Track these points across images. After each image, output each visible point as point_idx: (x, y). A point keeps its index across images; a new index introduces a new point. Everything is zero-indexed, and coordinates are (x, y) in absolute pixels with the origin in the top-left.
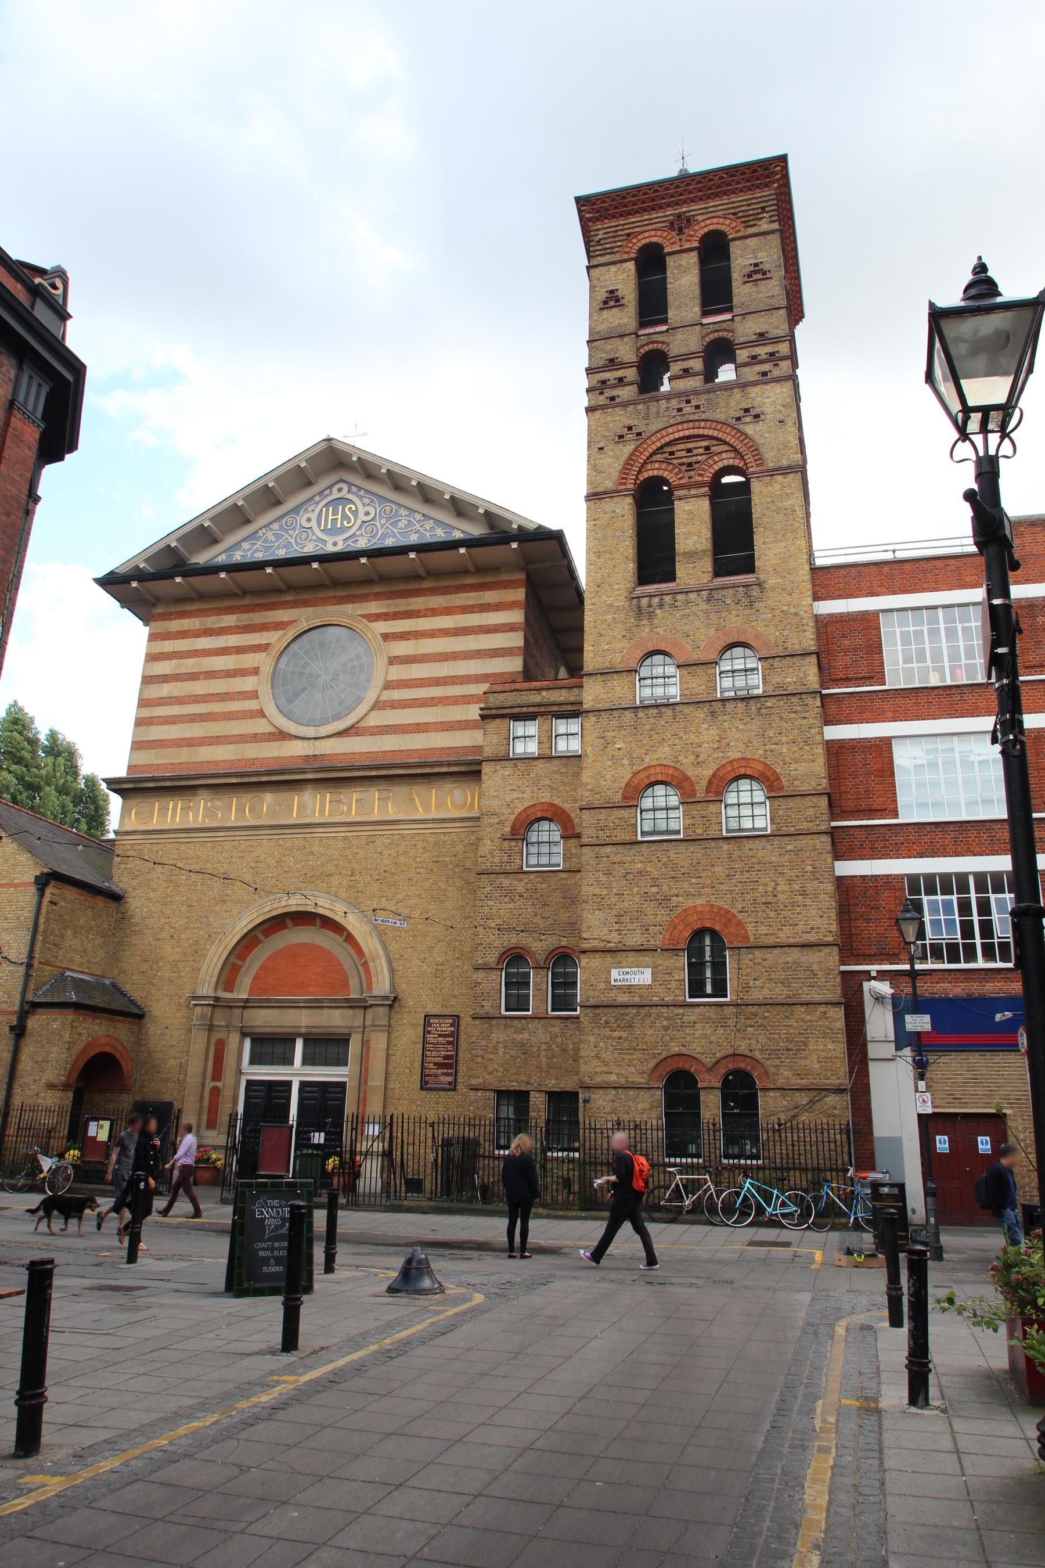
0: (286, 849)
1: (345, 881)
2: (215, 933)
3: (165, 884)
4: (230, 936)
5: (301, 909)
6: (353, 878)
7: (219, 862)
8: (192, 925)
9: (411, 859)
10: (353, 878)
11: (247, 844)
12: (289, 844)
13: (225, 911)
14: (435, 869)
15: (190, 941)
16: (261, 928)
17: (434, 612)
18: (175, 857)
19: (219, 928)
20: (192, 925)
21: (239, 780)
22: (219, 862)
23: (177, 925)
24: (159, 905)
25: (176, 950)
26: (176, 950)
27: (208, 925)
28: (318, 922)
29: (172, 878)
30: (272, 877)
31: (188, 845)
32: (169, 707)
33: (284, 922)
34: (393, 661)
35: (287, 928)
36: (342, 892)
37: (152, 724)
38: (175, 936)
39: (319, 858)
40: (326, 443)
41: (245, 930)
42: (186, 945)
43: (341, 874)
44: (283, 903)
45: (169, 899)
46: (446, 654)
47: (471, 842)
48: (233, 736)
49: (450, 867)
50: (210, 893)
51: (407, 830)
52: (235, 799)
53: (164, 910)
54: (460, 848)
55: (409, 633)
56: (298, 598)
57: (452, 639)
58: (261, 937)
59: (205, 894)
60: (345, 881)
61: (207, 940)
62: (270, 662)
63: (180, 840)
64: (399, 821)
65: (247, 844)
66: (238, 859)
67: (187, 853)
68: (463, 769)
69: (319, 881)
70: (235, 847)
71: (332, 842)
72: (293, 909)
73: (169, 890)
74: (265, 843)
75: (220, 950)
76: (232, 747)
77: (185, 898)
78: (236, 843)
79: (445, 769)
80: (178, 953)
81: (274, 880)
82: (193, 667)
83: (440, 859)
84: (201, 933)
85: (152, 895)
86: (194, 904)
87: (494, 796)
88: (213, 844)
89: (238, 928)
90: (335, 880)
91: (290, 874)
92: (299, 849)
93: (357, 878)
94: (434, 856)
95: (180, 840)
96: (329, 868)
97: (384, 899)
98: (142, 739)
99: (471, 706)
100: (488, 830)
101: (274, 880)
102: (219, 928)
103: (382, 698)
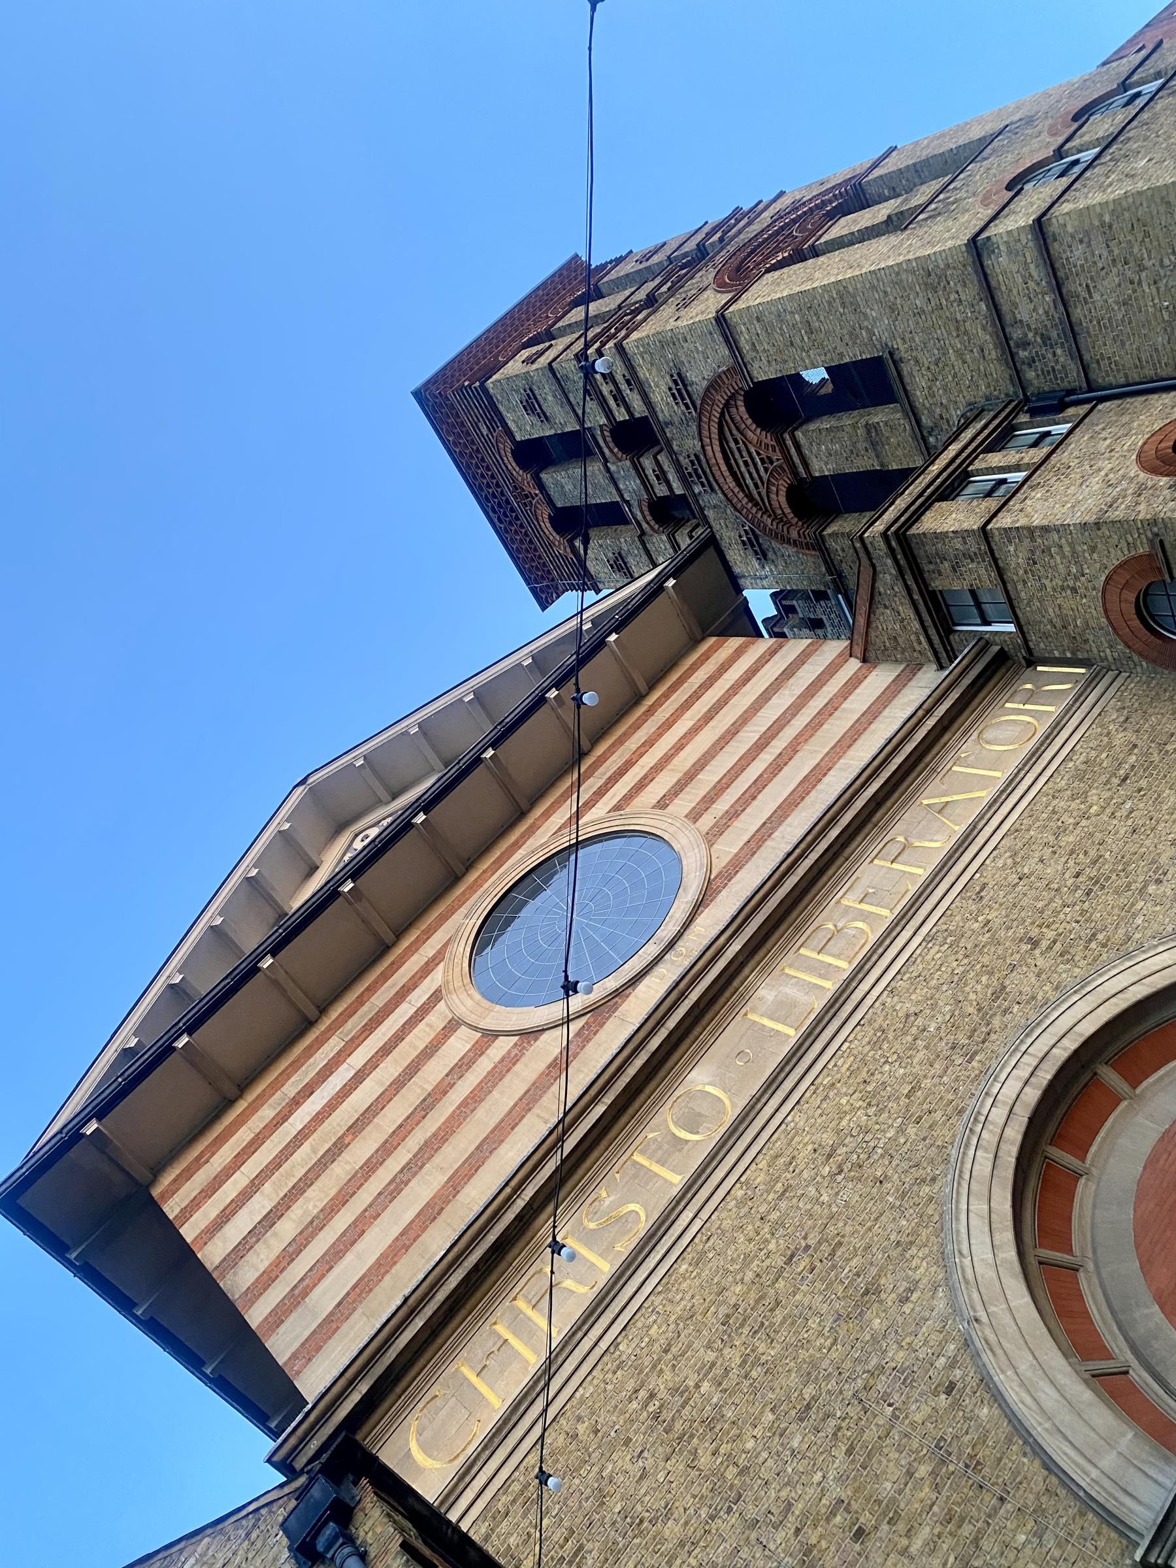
0: (852, 1072)
1: (1040, 962)
2: (952, 1364)
3: (677, 1465)
4: (998, 1309)
5: (1046, 1075)
6: (1044, 944)
7: (748, 1259)
8: (871, 1435)
9: (1084, 823)
10: (1044, 944)
11: (763, 1164)
12: (845, 1064)
13: (904, 1300)
14: (1143, 783)
15: (923, 1470)
16: (1028, 1238)
17: (650, 743)
18: (631, 1385)
19: (942, 1345)
20: (871, 1435)
21: (608, 1099)
22: (748, 1259)
23: (836, 1491)
24: (727, 1524)
25: (917, 1545)
26: (917, 1545)
27: (906, 1377)
28: (1110, 1076)
29: (678, 1426)
30: (901, 1130)
31: (632, 1331)
32: (321, 1235)
33: (1050, 1165)
34: (662, 804)
35: (1076, 1176)
36: (1064, 972)
37: (305, 1294)
38: (866, 1520)
39: (933, 1007)
40: (301, 788)
41: (1011, 1254)
42: (926, 1492)
43: (1013, 967)
44: (999, 1115)
45: (730, 1473)
46: (728, 731)
47: (1122, 719)
48: (510, 1112)
49: (1156, 757)
50: (813, 1323)
51: (1012, 813)
52: (637, 1158)
53: (751, 1512)
54: (1119, 739)
55: (645, 777)
56: (423, 927)
57: (712, 723)
58: (1065, 1158)
59: (804, 1344)
60: (1040, 962)
61: (956, 1405)
62: (463, 996)
63: (603, 1345)
64: (973, 825)
65: (763, 1164)
66: (783, 1205)
67: (652, 1342)
68: (954, 695)
69: (996, 1022)
70: (740, 1204)
71: (915, 970)
72: (1032, 1095)
73: (704, 1460)
74: (798, 1119)
75: (1025, 1364)
76: (529, 1119)
77: (771, 1417)
78: (739, 1193)
79: (931, 722)
80: (932, 1547)
81: (911, 1130)
82: (314, 1152)
83: (1122, 772)
84: (918, 1418)
85: (672, 1530)
86: (808, 1392)
87: (1073, 507)
88: (688, 1256)
89: (986, 1273)
90: (1022, 982)
91: (927, 1083)
92: (875, 1044)
93: (1051, 935)
94: (1108, 782)
95: (603, 1345)
96: (977, 990)
97: (1152, 888)
98: (307, 1334)
99: (843, 706)
100: (1142, 507)
101: (911, 1130)
102: (942, 1345)
103: (705, 829)
